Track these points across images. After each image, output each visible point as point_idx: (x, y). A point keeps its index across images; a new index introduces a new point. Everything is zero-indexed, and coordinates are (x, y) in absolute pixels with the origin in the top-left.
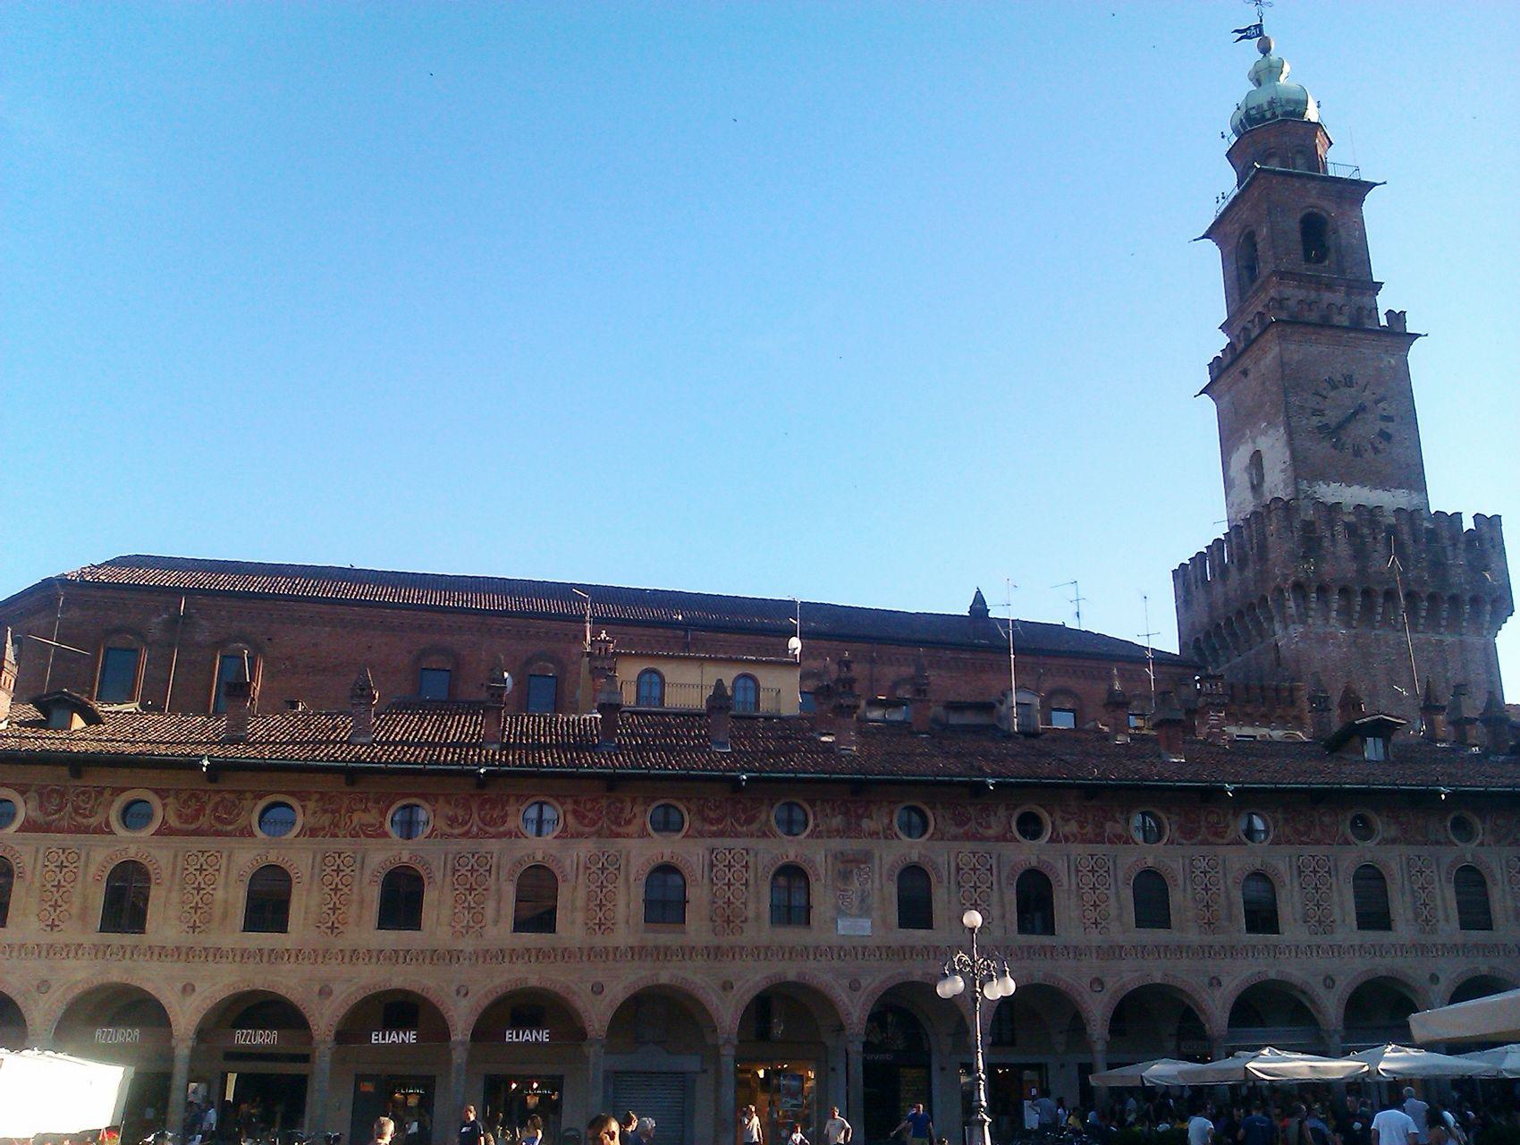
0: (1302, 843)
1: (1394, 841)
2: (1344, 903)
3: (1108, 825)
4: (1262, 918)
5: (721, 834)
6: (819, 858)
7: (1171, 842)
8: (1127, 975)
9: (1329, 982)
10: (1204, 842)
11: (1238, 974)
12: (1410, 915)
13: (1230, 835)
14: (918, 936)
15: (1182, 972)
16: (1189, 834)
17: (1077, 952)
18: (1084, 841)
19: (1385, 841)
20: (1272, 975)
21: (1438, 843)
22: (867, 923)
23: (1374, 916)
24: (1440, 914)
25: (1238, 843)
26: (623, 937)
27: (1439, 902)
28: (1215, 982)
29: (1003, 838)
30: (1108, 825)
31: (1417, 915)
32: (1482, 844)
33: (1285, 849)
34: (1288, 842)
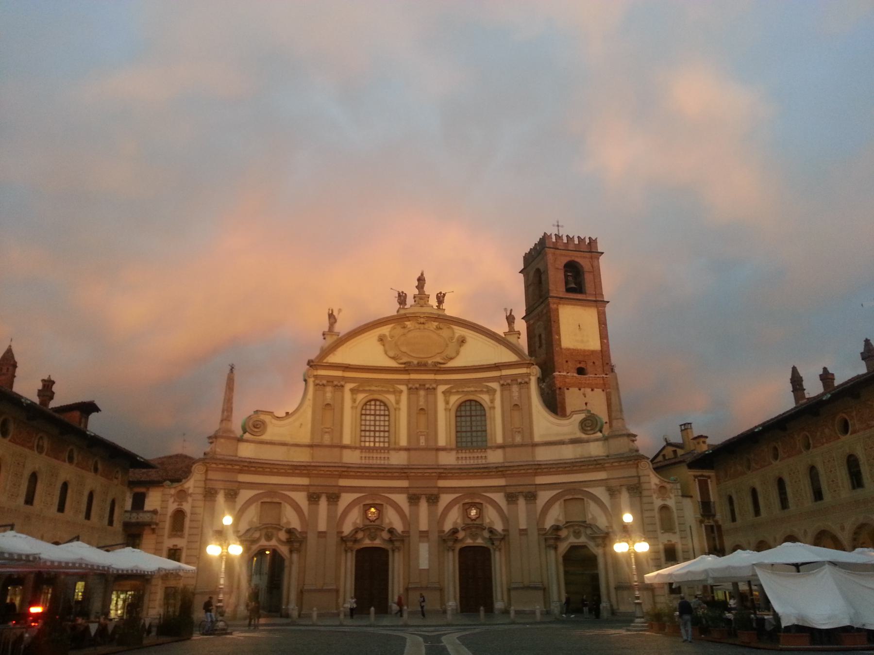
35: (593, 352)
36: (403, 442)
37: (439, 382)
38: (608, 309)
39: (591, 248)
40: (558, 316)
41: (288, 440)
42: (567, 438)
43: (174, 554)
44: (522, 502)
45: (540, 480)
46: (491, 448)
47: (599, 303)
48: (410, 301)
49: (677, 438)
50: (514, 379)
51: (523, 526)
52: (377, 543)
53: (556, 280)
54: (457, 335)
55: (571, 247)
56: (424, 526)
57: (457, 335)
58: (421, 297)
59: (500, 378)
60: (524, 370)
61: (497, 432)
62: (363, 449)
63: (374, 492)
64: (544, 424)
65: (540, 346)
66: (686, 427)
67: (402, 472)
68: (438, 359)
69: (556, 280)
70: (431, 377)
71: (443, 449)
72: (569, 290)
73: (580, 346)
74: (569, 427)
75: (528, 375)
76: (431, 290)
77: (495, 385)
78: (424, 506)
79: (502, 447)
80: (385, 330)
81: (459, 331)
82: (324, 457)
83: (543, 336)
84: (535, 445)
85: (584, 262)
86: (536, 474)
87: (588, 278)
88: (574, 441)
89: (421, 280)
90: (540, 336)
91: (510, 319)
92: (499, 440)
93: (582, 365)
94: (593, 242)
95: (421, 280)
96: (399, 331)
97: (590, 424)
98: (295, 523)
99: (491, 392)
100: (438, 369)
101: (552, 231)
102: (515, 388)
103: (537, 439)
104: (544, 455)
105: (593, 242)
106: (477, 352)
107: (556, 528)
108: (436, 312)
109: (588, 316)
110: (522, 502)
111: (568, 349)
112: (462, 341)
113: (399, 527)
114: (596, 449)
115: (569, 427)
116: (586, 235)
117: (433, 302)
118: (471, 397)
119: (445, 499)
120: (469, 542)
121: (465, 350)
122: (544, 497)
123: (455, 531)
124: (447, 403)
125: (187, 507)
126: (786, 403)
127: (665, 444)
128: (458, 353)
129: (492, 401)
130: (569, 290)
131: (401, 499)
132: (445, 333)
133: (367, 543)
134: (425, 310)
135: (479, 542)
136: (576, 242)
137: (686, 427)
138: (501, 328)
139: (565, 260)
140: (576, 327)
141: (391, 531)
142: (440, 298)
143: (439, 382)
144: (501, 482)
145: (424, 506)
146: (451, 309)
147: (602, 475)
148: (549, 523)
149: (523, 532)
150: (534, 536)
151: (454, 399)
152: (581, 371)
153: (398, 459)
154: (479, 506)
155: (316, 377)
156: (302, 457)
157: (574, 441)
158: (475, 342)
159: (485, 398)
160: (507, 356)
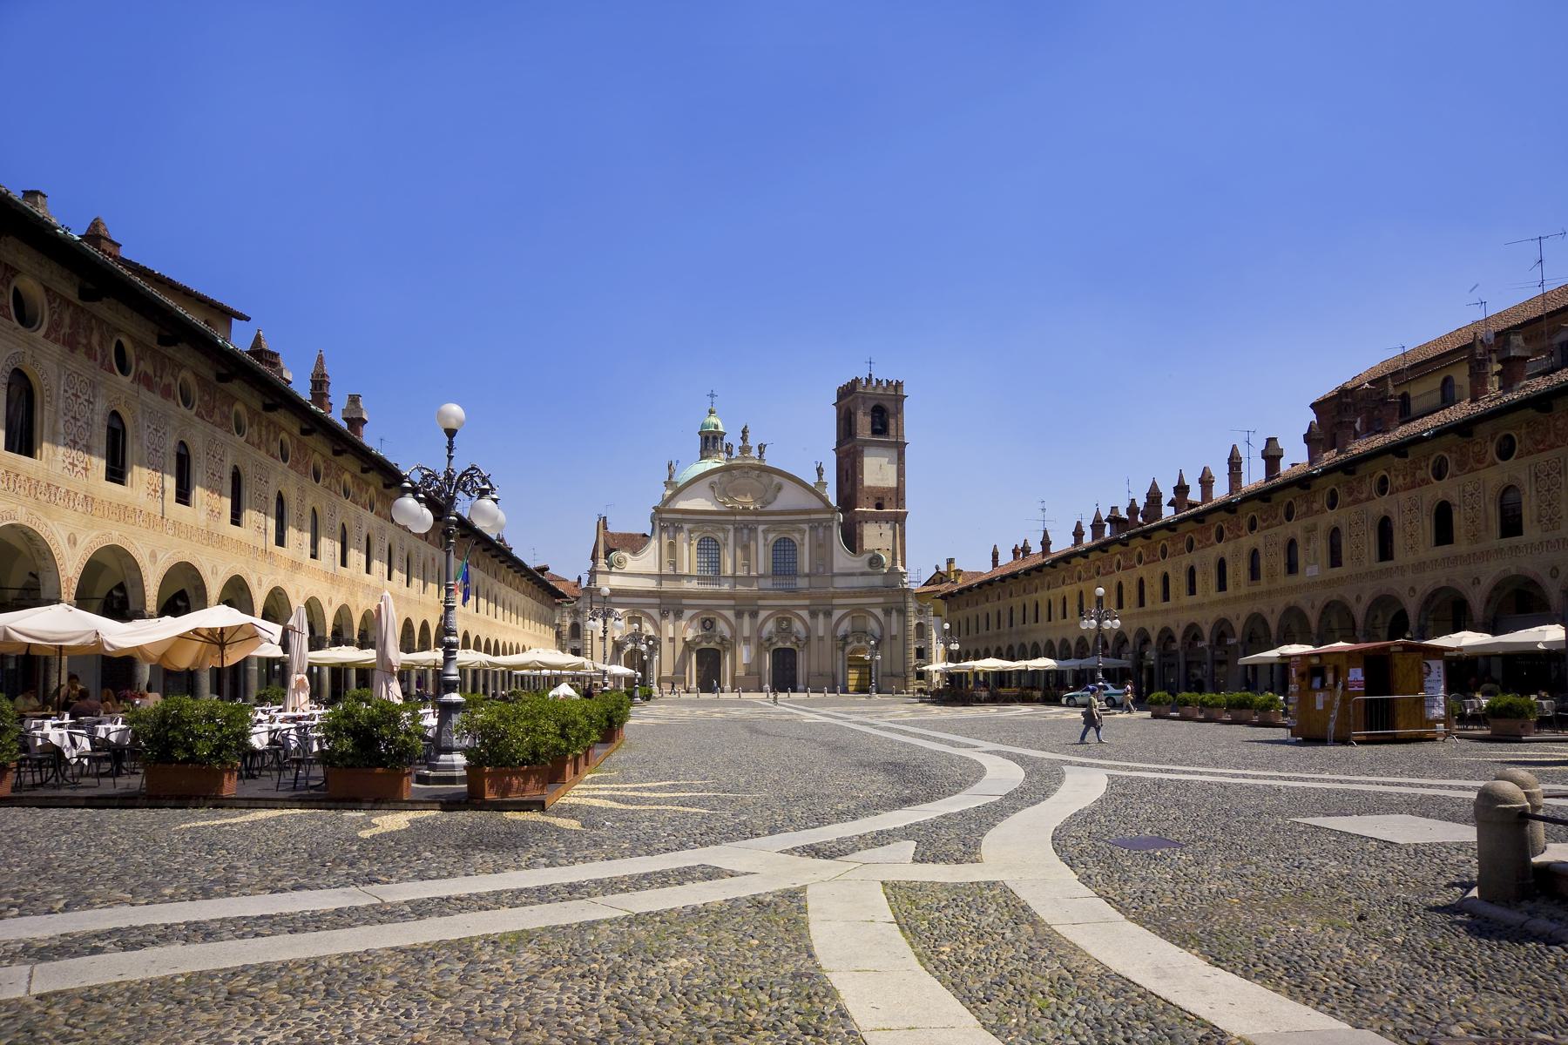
4: (1511, 525)
5: (1268, 527)
7: (1452, 476)
8: (1429, 581)
10: (1472, 470)
13: (1488, 459)
16: (1461, 465)
17: (1402, 570)
18: (1407, 489)
20: (1514, 572)
22: (1316, 568)
25: (1495, 464)
26: (1244, 590)
28: (1477, 581)
29: (1368, 499)
33: (1527, 460)
34: (1529, 453)
35: (890, 489)
36: (729, 572)
37: (759, 523)
41: (643, 571)
43: (576, 652)
44: (821, 616)
45: (835, 602)
47: (900, 447)
48: (736, 452)
49: (943, 569)
50: (820, 522)
51: (821, 633)
52: (712, 645)
53: (863, 423)
55: (880, 391)
56: (746, 633)
58: (745, 449)
59: (809, 521)
61: (805, 564)
62: (698, 578)
63: (708, 609)
64: (842, 558)
66: (950, 561)
67: (730, 596)
72: (875, 432)
73: (881, 484)
76: (753, 442)
77: (806, 527)
78: (746, 618)
79: (808, 575)
80: (715, 478)
81: (777, 479)
82: (668, 586)
84: (834, 575)
85: (890, 406)
87: (892, 421)
88: (863, 574)
91: (820, 471)
92: (807, 570)
94: (899, 385)
96: (726, 477)
98: (652, 633)
101: (863, 375)
102: (821, 530)
104: (840, 583)
105: (899, 385)
106: (789, 498)
107: (845, 637)
110: (821, 616)
112: (779, 488)
113: (727, 633)
114: (877, 581)
116: (893, 378)
117: (755, 453)
119: (763, 614)
120: (780, 645)
122: (837, 614)
123: (769, 639)
125: (579, 621)
126: (985, 567)
131: (730, 614)
132: (765, 478)
133: (704, 645)
135: (788, 645)
137: (950, 561)
138: (811, 480)
139: (872, 404)
141: (723, 639)
142: (761, 448)
143: (759, 523)
144: (807, 602)
145: (746, 618)
146: (769, 461)
147: (881, 600)
148: (840, 632)
149: (821, 639)
150: (828, 641)
151: (771, 536)
152: (879, 506)
153: (726, 587)
154: (789, 621)
155: (661, 520)
156: (650, 585)
157: (863, 574)
158: (789, 487)
159: (796, 537)
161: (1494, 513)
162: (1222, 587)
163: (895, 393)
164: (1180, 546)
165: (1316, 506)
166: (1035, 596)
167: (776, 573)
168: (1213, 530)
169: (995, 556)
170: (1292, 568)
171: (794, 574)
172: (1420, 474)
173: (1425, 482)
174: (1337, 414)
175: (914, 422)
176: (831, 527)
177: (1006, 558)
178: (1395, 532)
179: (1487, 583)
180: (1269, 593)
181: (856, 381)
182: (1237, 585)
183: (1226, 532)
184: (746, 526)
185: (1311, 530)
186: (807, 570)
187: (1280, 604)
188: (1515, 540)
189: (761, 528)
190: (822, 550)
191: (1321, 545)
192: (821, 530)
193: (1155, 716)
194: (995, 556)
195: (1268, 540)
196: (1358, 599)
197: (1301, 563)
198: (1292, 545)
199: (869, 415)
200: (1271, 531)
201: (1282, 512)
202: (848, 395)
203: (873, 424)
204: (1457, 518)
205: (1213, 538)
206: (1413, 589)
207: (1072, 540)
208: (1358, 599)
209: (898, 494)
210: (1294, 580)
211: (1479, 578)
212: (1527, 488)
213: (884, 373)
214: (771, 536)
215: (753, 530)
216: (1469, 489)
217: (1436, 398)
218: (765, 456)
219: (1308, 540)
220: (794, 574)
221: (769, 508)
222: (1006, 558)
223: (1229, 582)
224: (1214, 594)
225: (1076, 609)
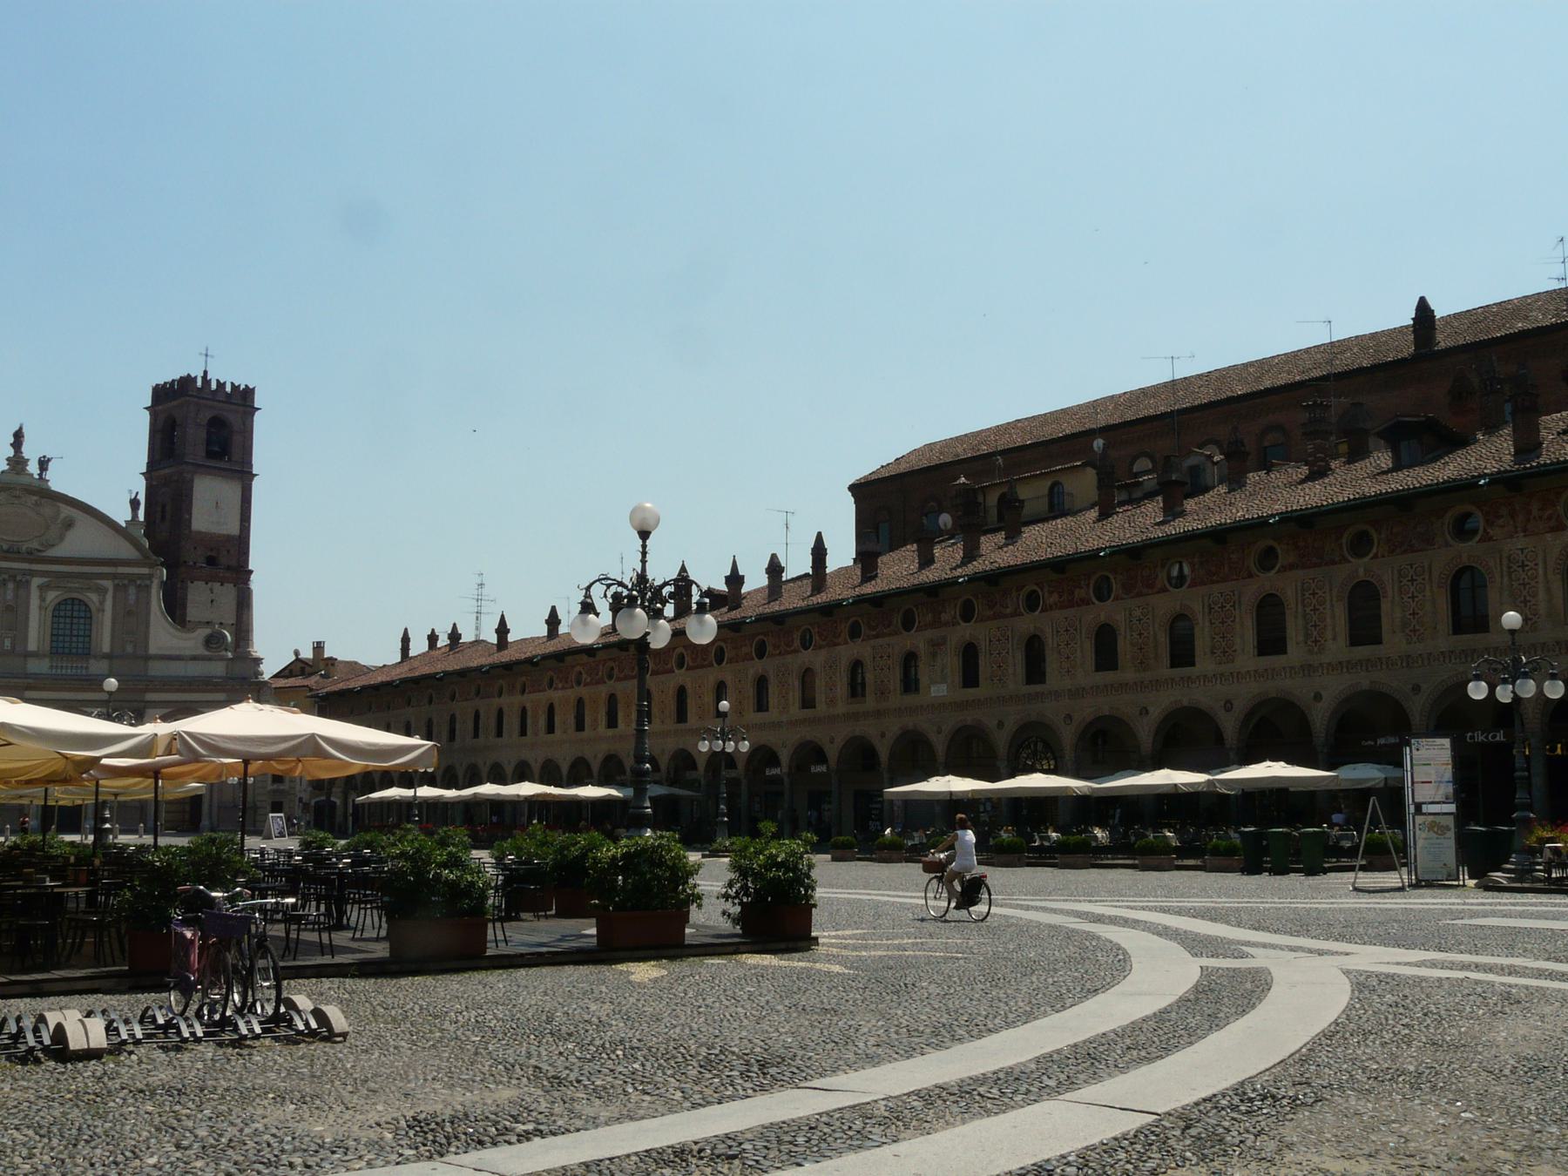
0: (1213, 582)
1: (1291, 567)
2: (1246, 633)
3: (1077, 591)
4: (1182, 654)
5: (877, 637)
6: (921, 645)
7: (1116, 599)
8: (1088, 709)
9: (1228, 705)
10: (1140, 595)
11: (1161, 703)
12: (1301, 638)
14: (971, 692)
15: (1203, 696)
18: (1061, 608)
19: (1284, 569)
20: (1185, 703)
21: (1333, 563)
22: (944, 687)
23: (1271, 642)
24: (1329, 635)
25: (1164, 590)
26: (841, 708)
27: (1329, 620)
28: (1144, 711)
29: (1016, 614)
30: (1077, 591)
31: (1307, 635)
32: (1376, 556)
37: (33, 573)
38: (256, 485)
39: (243, 399)
40: (191, 489)
42: (188, 653)
45: (151, 696)
46: (95, 657)
47: (244, 475)
49: (307, 654)
50: (132, 579)
53: (194, 438)
54: (62, 516)
57: (62, 516)
59: (114, 576)
60: (145, 571)
65: (163, 518)
66: (318, 647)
68: (35, 545)
69: (194, 438)
70: (25, 566)
71: (35, 655)
72: (210, 455)
73: (214, 529)
74: (191, 643)
75: (150, 577)
76: (31, 452)
77: (108, 584)
79: (108, 657)
81: (66, 511)
83: (168, 508)
86: (147, 690)
88: (194, 658)
89: (18, 436)
90: (164, 507)
92: (106, 648)
93: (214, 554)
95: (18, 436)
97: (213, 641)
99: (102, 591)
100: (32, 556)
101: (197, 373)
102: (132, 590)
103: (152, 650)
108: (37, 484)
109: (231, 490)
111: (200, 533)
112: (69, 524)
114: (217, 669)
115: (191, 643)
116: (242, 382)
117: (33, 468)
118: (75, 595)
121: (71, 535)
124: (43, 599)
127: (293, 658)
128: (61, 538)
129: (102, 602)
130: (210, 455)
132: (47, 510)
134: (23, 480)
136: (228, 389)
137: (318, 647)
140: (208, 505)
142: (44, 464)
143: (33, 573)
146: (58, 481)
151: (52, 596)
152: (211, 561)
159: (93, 598)
160: (126, 551)
161: (1163, 639)
162: (808, 702)
163: (243, 399)
164: (745, 650)
165: (945, 617)
166: (496, 702)
167: (56, 652)
168: (797, 636)
169: (406, 640)
170: (910, 684)
171: (87, 654)
172: (1079, 593)
173: (1085, 602)
174: (894, 503)
175: (270, 443)
176: (148, 587)
177: (419, 646)
178: (1048, 652)
179: (1156, 713)
180: (878, 714)
181: (187, 381)
182: (832, 702)
183: (816, 638)
184: (13, 578)
185: (936, 645)
186: (106, 648)
187: (894, 727)
188: (1186, 671)
189: (36, 582)
190: (132, 621)
191: (951, 662)
192: (132, 590)
193: (834, 859)
194: (406, 640)
195: (878, 652)
196: (1001, 724)
197: (924, 680)
198: (910, 659)
199: (201, 431)
200: (880, 641)
201: (897, 620)
202: (162, 394)
203: (209, 443)
204: (1124, 646)
205: (797, 643)
206: (1069, 717)
207: (543, 630)
208: (1001, 724)
209: (241, 543)
210: (910, 699)
211: (1151, 703)
212: (1200, 617)
213: (226, 372)
214: (52, 596)
215: (22, 585)
216: (1137, 613)
217: (1042, 506)
218: (48, 475)
219: (934, 655)
220: (87, 654)
221: (52, 553)
222: (419, 646)
223: (820, 698)
224: (795, 711)
225: (572, 720)
